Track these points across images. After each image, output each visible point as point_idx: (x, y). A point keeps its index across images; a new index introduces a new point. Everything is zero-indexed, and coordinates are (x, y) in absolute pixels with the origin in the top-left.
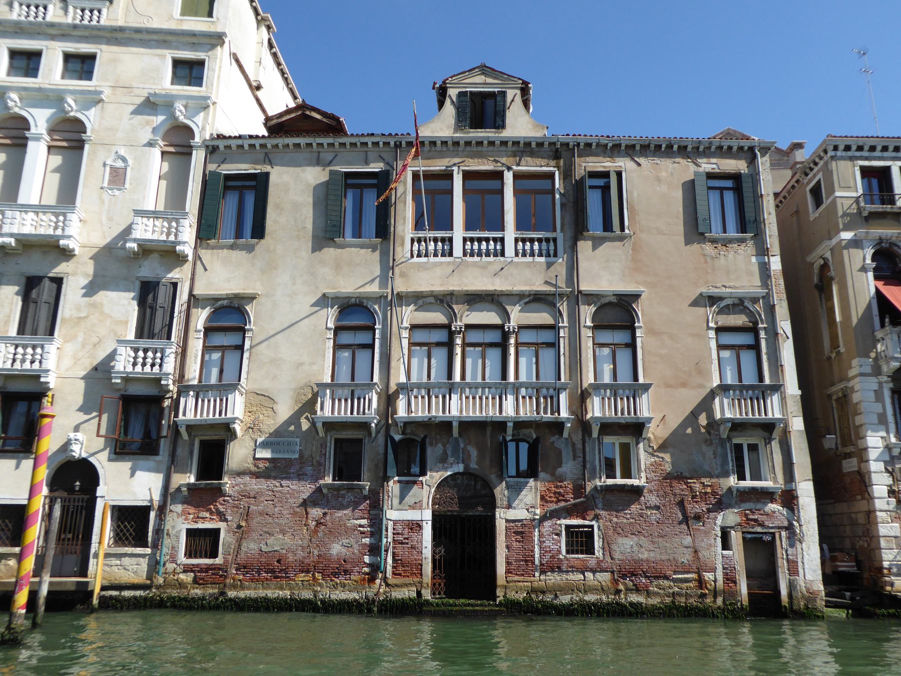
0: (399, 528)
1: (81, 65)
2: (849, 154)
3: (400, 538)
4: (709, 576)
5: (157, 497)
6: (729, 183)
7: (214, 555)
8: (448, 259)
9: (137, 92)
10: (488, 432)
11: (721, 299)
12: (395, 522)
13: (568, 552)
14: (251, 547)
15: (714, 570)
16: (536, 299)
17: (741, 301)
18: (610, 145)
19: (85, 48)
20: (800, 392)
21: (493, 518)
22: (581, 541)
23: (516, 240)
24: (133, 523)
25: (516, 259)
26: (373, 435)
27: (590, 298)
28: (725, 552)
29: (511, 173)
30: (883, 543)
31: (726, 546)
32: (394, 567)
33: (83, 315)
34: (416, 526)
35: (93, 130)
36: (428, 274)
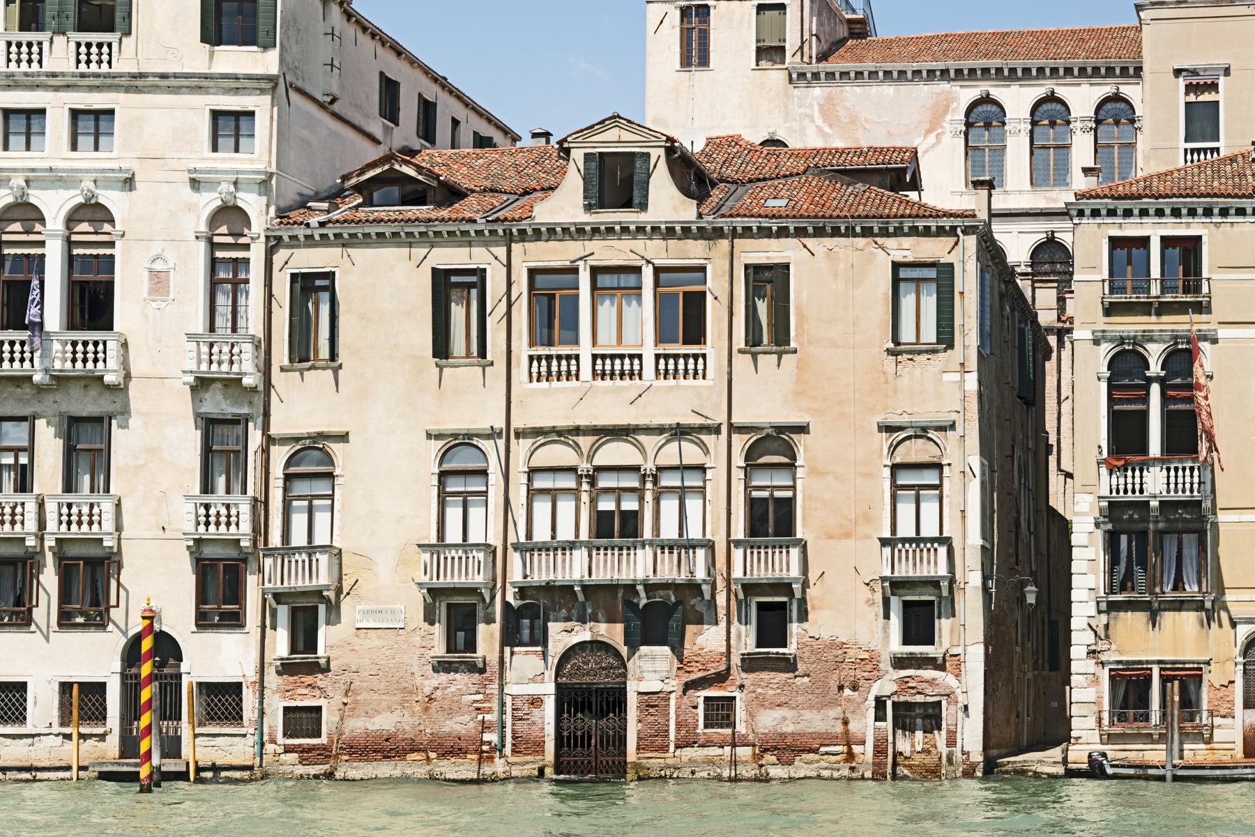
0: (519, 704)
1: (91, 124)
2: (1098, 220)
3: (520, 714)
4: (857, 749)
5: (251, 674)
6: (932, 273)
7: (320, 736)
8: (573, 383)
9: (174, 164)
10: (620, 595)
11: (900, 428)
12: (514, 697)
13: (706, 726)
14: (357, 726)
15: (863, 743)
16: (680, 432)
17: (924, 429)
18: (774, 228)
19: (98, 100)
20: (981, 542)
21: (623, 692)
22: (720, 712)
23: (658, 357)
24: (222, 701)
25: (656, 383)
26: (488, 600)
27: (742, 429)
28: (878, 724)
29: (651, 266)
30: (1075, 710)
31: (880, 716)
32: (513, 745)
33: (141, 462)
34: (536, 701)
35: (123, 220)
36: (548, 404)
